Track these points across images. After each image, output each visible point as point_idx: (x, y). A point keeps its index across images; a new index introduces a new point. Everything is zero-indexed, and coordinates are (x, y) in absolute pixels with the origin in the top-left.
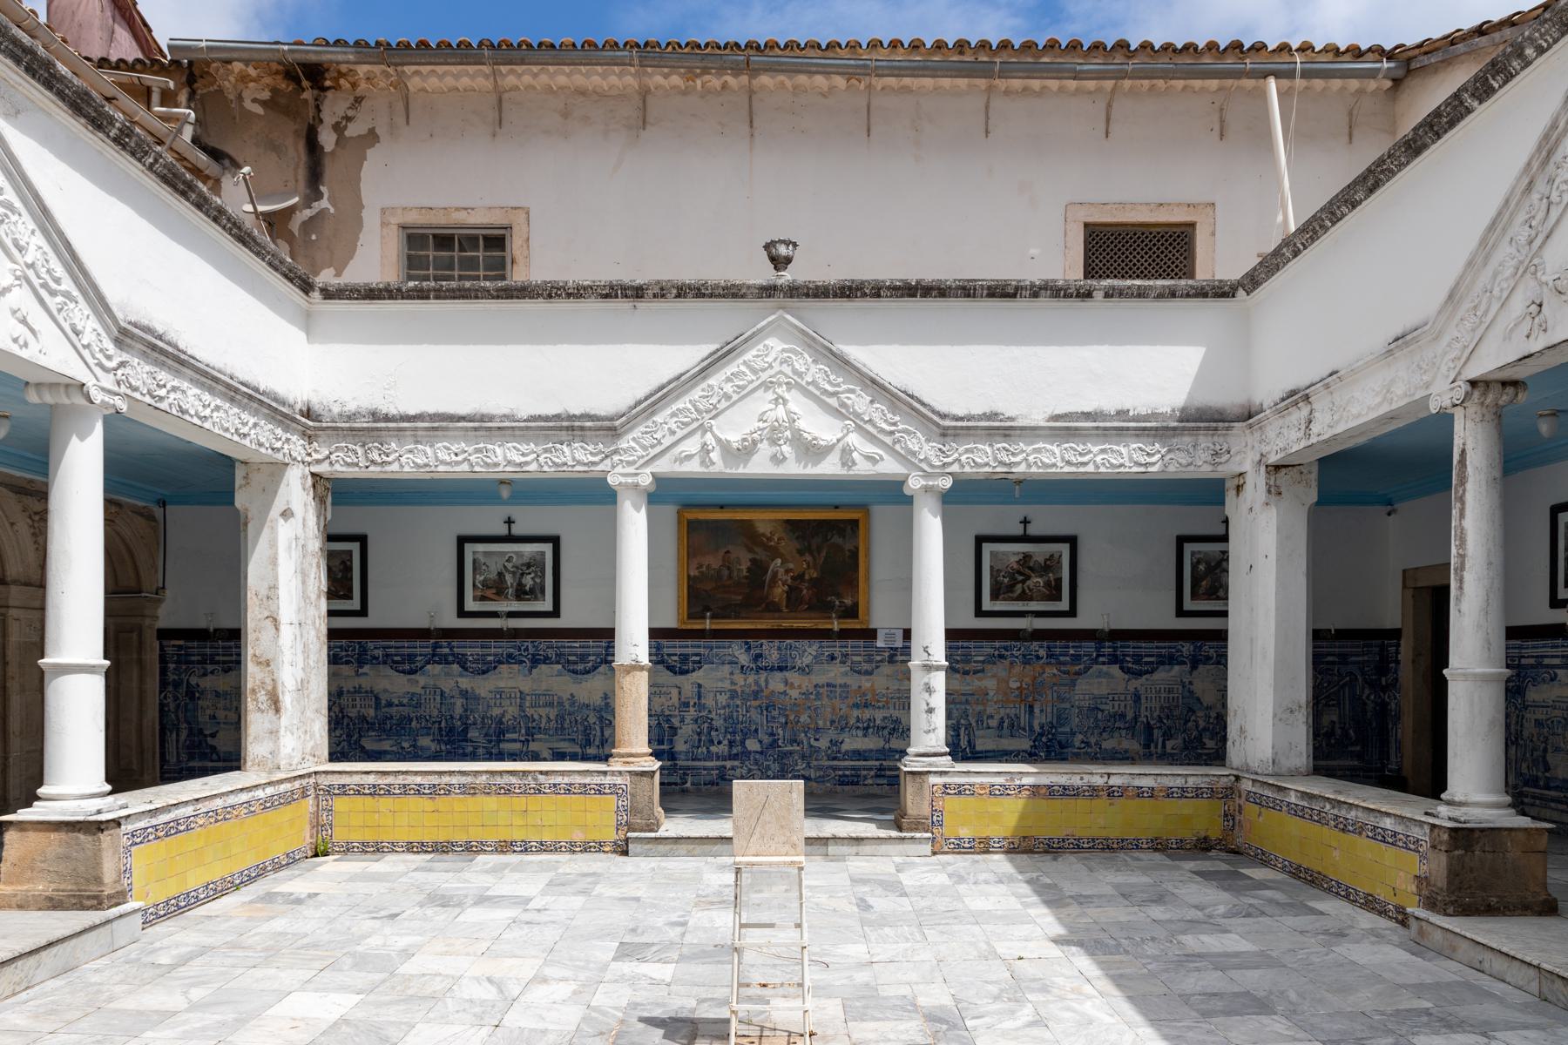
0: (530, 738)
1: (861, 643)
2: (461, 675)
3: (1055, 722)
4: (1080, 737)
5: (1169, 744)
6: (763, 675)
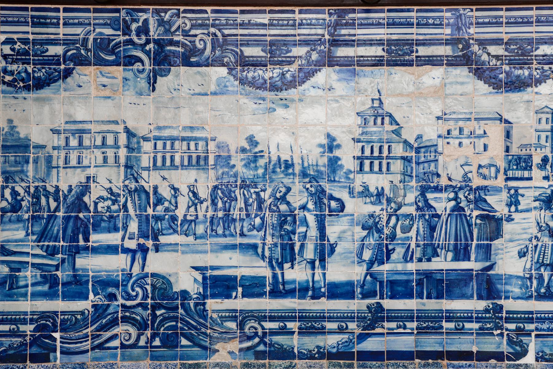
0: (150, 243)
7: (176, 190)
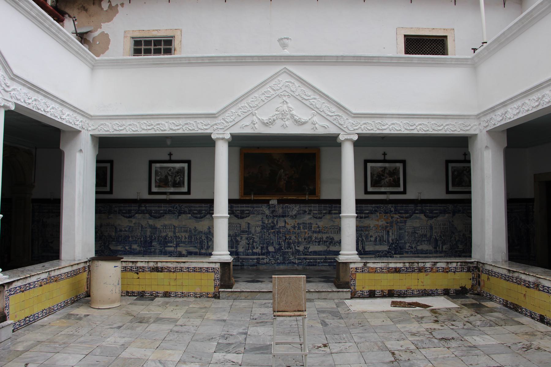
1: (317, 205)
2: (150, 219)
3: (398, 239)
4: (408, 244)
5: (444, 247)
6: (276, 219)
7: (182, 236)
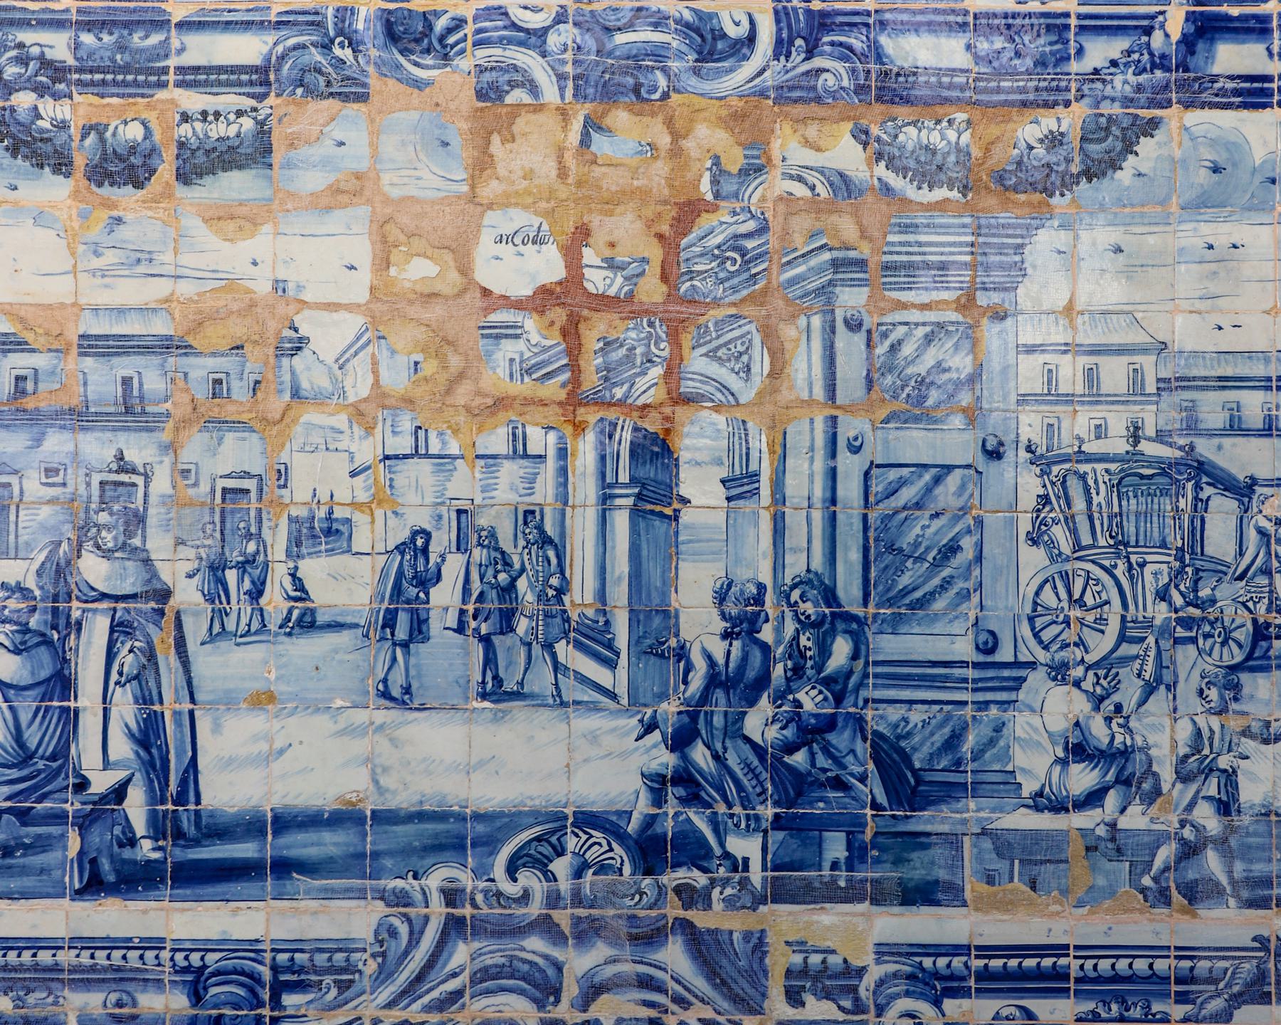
3: (849, 589)
